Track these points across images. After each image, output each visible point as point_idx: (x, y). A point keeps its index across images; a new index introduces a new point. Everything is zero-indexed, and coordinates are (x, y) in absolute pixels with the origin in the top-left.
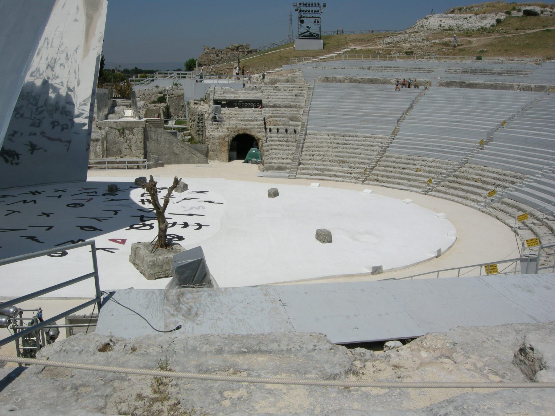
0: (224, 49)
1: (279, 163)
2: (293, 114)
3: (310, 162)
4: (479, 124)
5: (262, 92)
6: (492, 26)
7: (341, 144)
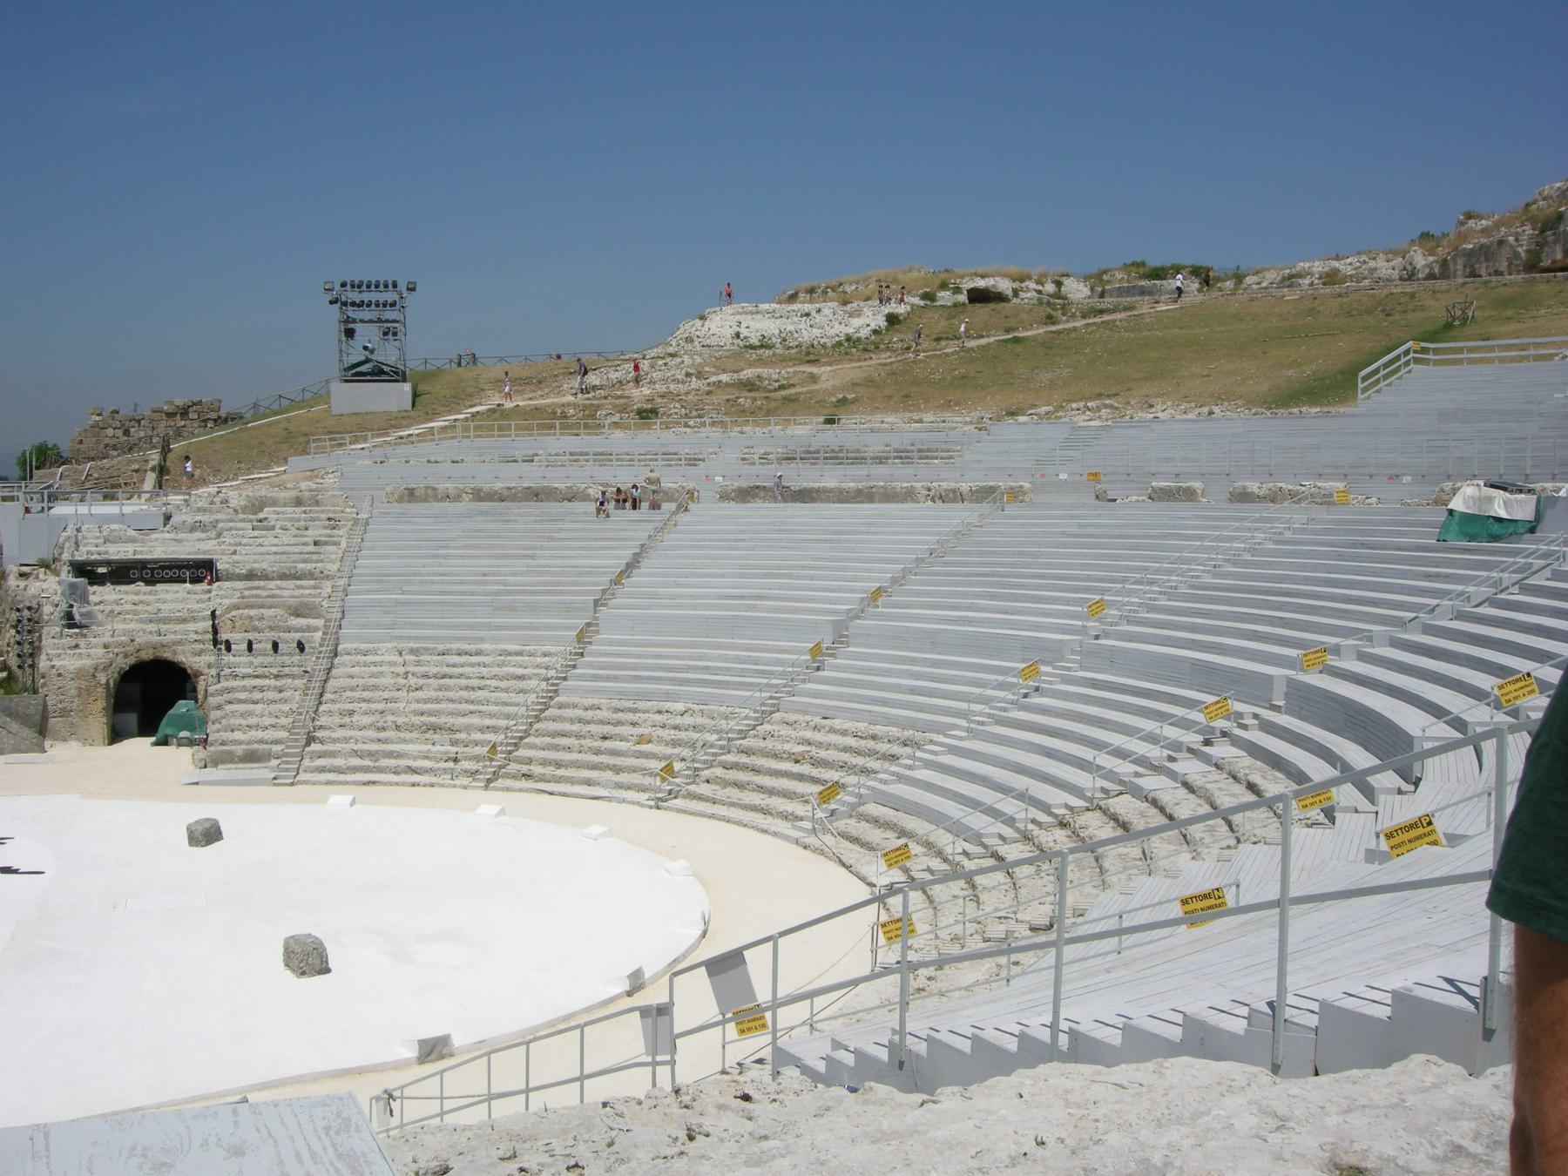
0: (147, 413)
1: (249, 743)
2: (302, 596)
3: (340, 733)
4: (812, 600)
5: (219, 535)
6: (875, 332)
7: (435, 676)
